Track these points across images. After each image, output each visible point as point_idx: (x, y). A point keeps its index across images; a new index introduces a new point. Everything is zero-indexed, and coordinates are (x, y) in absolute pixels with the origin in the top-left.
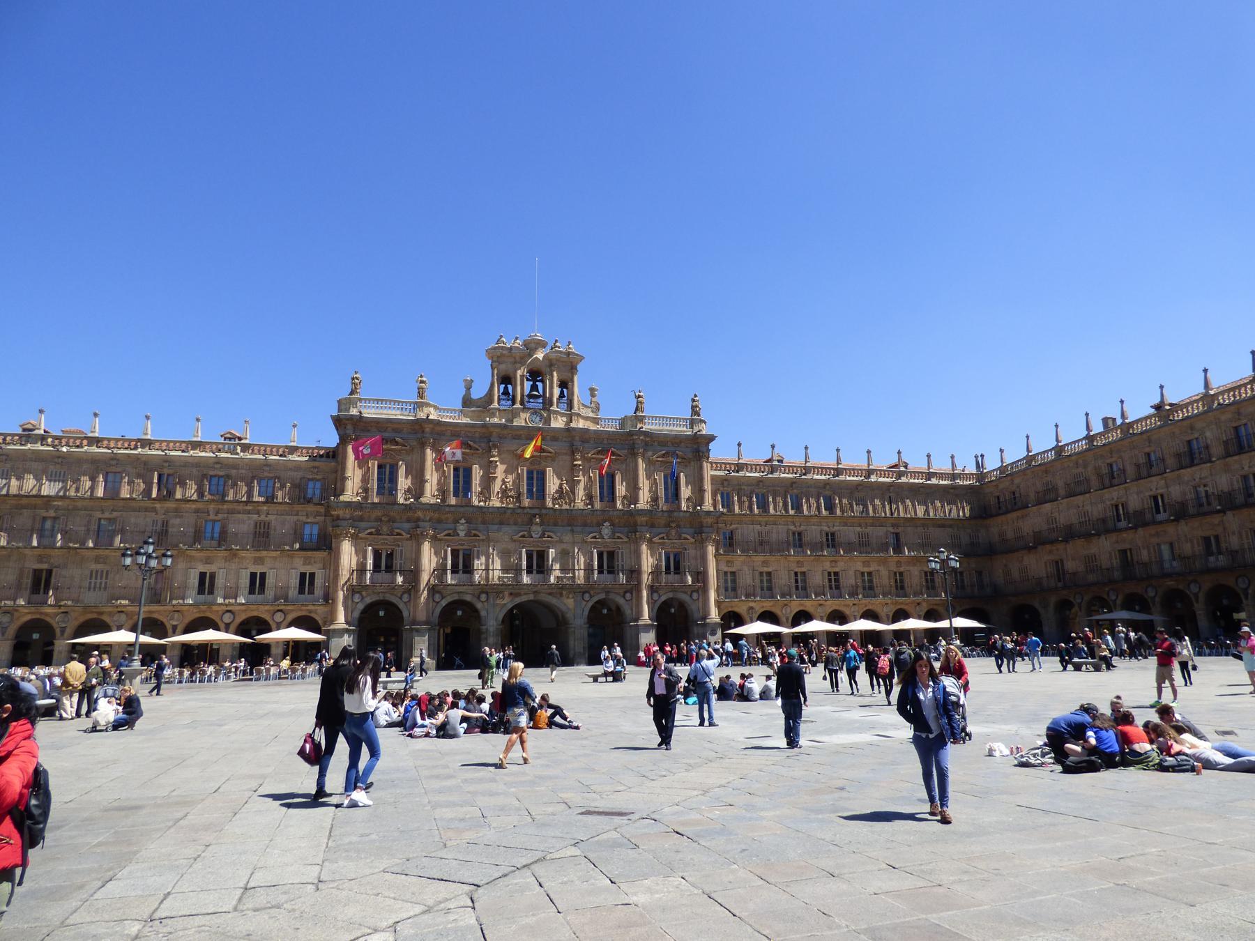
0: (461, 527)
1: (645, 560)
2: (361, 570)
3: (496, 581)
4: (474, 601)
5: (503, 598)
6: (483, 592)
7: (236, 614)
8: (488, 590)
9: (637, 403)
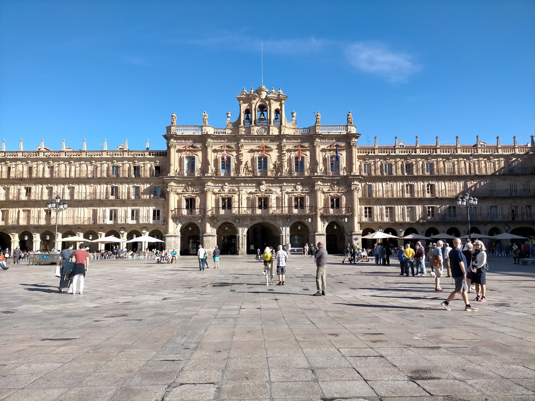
0: (226, 187)
1: (320, 202)
2: (179, 208)
3: (244, 213)
4: (233, 223)
5: (247, 221)
6: (237, 219)
7: (126, 229)
8: (240, 218)
9: (317, 119)
